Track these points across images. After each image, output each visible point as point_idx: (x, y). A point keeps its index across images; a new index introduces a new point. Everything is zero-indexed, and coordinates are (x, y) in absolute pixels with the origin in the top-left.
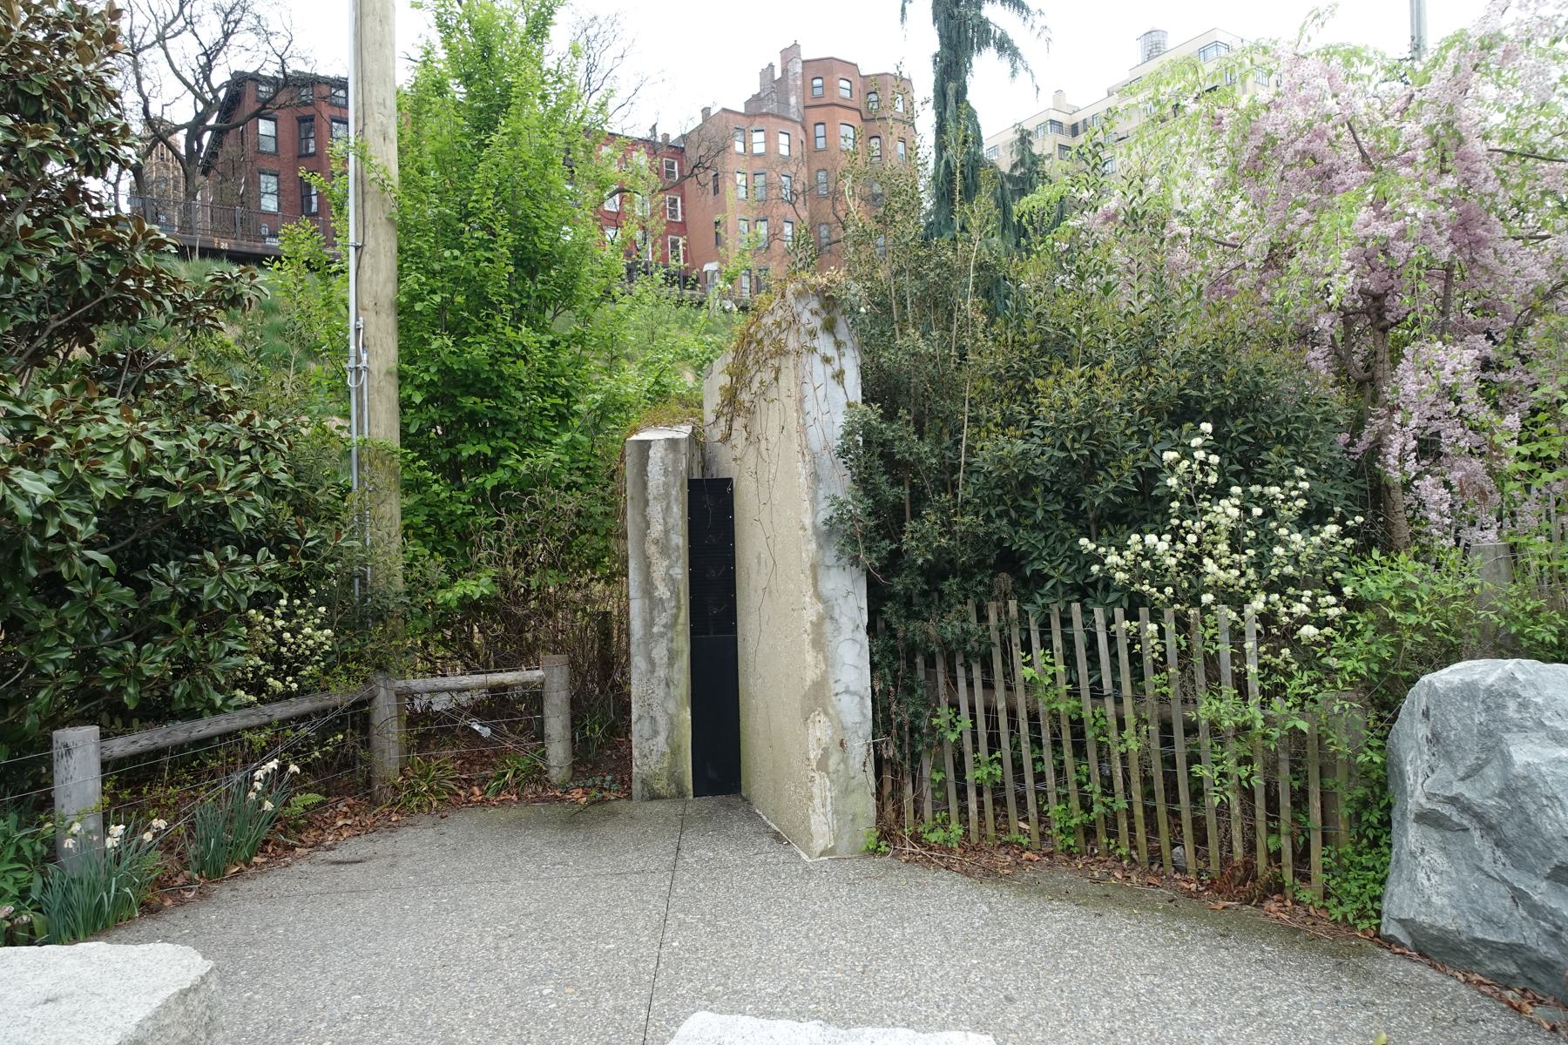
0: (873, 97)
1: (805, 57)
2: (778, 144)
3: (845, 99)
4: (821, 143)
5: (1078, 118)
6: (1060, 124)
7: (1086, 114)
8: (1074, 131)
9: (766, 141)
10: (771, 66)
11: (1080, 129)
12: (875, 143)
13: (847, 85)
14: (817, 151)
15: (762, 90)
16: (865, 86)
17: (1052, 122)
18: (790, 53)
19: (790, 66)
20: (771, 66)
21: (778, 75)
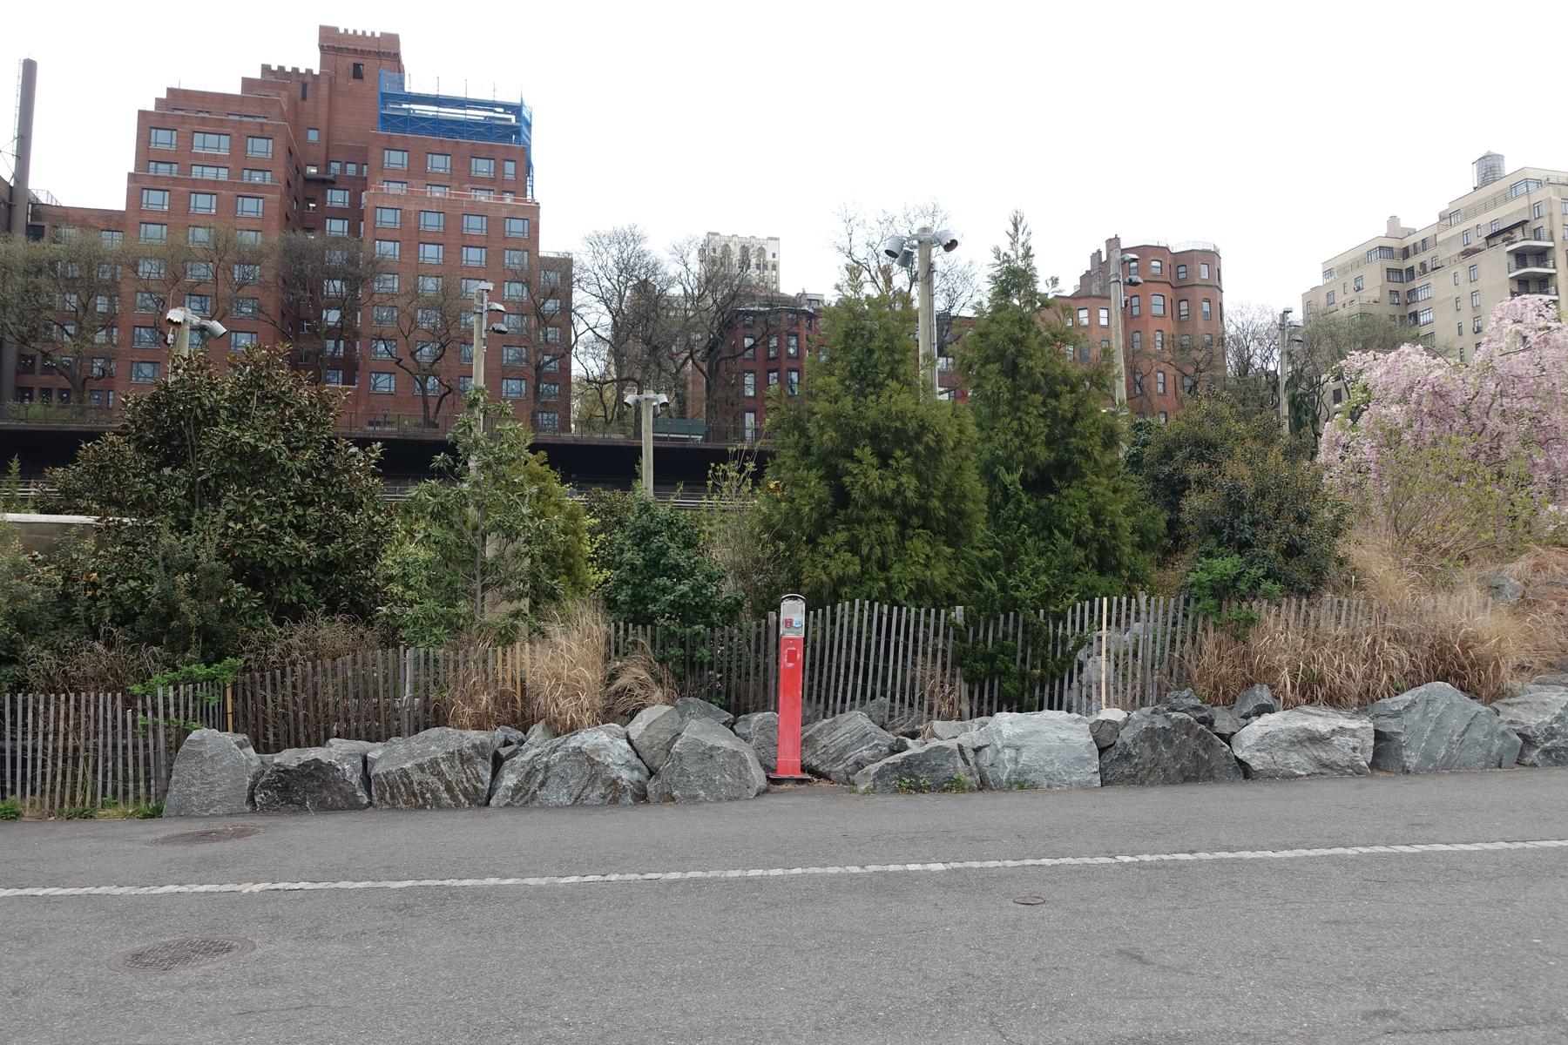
0: (1182, 269)
1: (1122, 247)
2: (1098, 318)
3: (1156, 276)
4: (1136, 311)
5: (1409, 241)
6: (1391, 249)
7: (1417, 239)
8: (1406, 253)
9: (1089, 316)
10: (1099, 252)
12: (1184, 306)
13: (1158, 264)
14: (1133, 317)
15: (1092, 270)
16: (1176, 261)
17: (1381, 248)
18: (1113, 243)
19: (1111, 254)
20: (1099, 252)
21: (1104, 258)
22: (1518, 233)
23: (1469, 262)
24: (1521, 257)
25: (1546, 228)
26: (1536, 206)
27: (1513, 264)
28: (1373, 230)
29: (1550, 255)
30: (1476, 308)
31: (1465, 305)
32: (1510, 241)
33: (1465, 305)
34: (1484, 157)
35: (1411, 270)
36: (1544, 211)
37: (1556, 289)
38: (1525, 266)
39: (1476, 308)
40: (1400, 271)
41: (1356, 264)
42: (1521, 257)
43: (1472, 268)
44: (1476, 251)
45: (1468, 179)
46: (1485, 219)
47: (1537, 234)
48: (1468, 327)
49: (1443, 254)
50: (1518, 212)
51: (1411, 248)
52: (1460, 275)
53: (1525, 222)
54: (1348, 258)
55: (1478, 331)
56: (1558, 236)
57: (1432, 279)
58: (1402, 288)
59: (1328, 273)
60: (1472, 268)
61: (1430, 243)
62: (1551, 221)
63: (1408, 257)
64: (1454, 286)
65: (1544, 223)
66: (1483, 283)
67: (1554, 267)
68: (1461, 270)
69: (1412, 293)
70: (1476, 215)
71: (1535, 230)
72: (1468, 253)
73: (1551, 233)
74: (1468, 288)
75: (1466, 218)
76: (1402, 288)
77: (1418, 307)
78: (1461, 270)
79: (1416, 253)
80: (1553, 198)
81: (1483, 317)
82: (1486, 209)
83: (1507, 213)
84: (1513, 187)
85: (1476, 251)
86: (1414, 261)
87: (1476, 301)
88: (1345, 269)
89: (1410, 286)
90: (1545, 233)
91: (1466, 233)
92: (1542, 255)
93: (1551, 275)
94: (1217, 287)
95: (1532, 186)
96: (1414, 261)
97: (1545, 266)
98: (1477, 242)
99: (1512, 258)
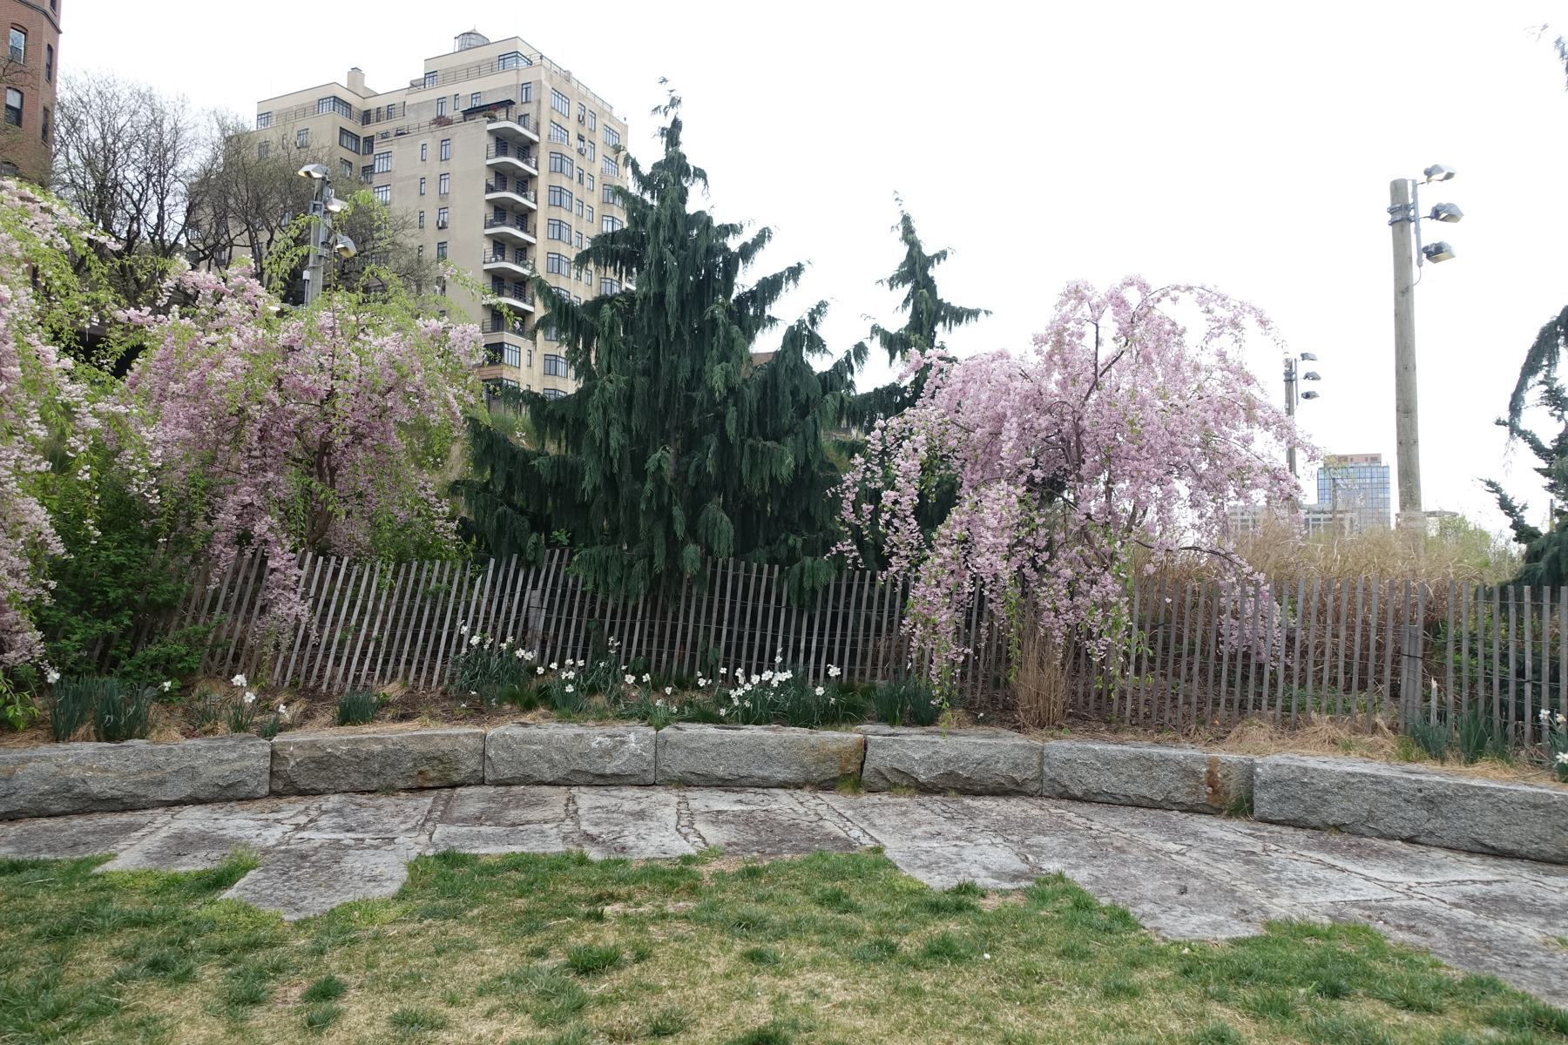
5: (372, 104)
6: (348, 105)
7: (382, 103)
8: (366, 117)
11: (373, 117)
22: (501, 114)
23: (441, 133)
24: (504, 142)
25: (533, 116)
26: (526, 87)
27: (493, 149)
28: (330, 73)
29: (533, 152)
30: (443, 196)
31: (431, 189)
32: (493, 119)
33: (431, 189)
34: (469, 34)
35: (369, 141)
36: (533, 95)
37: (536, 195)
38: (505, 154)
39: (443, 196)
40: (357, 138)
41: (303, 111)
42: (504, 142)
43: (445, 142)
44: (449, 122)
45: (450, 46)
46: (466, 89)
47: (522, 119)
48: (431, 219)
49: (409, 121)
50: (504, 89)
51: (374, 113)
52: (429, 148)
53: (510, 103)
54: (292, 103)
55: (443, 227)
56: (545, 128)
57: (395, 147)
58: (359, 161)
59: (264, 117)
60: (445, 142)
61: (398, 112)
62: (539, 109)
63: (368, 122)
64: (419, 162)
65: (529, 109)
66: (454, 166)
67: (537, 168)
68: (432, 141)
69: (368, 170)
70: (455, 81)
71: (520, 117)
72: (441, 121)
73: (537, 124)
74: (438, 168)
75: (444, 82)
76: (359, 161)
77: (377, 180)
78: (432, 141)
79: (378, 121)
80: (544, 82)
81: (450, 210)
82: (468, 77)
83: (493, 87)
84: (503, 58)
85: (449, 122)
86: (372, 130)
87: (445, 187)
88: (288, 115)
89: (368, 160)
90: (532, 124)
91: (441, 101)
92: (525, 148)
93: (531, 176)
94: (46, 14)
95: (522, 64)
96: (372, 130)
97: (527, 163)
98: (449, 112)
99: (491, 142)
